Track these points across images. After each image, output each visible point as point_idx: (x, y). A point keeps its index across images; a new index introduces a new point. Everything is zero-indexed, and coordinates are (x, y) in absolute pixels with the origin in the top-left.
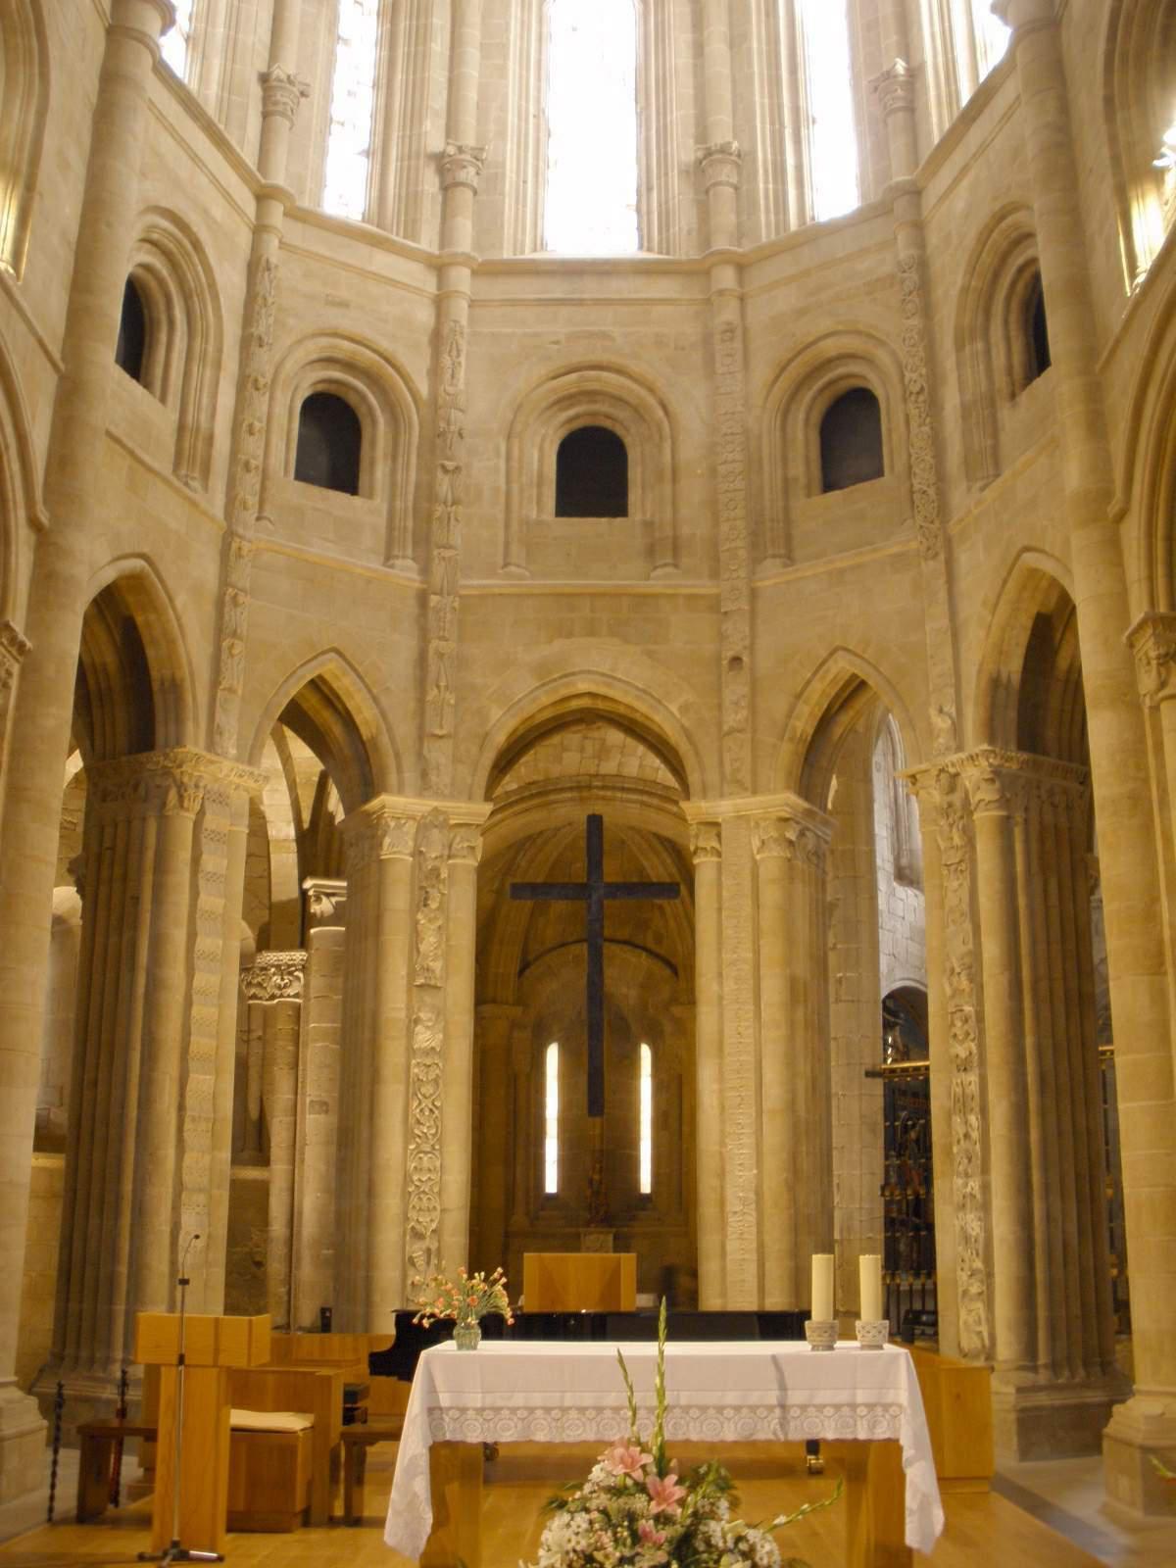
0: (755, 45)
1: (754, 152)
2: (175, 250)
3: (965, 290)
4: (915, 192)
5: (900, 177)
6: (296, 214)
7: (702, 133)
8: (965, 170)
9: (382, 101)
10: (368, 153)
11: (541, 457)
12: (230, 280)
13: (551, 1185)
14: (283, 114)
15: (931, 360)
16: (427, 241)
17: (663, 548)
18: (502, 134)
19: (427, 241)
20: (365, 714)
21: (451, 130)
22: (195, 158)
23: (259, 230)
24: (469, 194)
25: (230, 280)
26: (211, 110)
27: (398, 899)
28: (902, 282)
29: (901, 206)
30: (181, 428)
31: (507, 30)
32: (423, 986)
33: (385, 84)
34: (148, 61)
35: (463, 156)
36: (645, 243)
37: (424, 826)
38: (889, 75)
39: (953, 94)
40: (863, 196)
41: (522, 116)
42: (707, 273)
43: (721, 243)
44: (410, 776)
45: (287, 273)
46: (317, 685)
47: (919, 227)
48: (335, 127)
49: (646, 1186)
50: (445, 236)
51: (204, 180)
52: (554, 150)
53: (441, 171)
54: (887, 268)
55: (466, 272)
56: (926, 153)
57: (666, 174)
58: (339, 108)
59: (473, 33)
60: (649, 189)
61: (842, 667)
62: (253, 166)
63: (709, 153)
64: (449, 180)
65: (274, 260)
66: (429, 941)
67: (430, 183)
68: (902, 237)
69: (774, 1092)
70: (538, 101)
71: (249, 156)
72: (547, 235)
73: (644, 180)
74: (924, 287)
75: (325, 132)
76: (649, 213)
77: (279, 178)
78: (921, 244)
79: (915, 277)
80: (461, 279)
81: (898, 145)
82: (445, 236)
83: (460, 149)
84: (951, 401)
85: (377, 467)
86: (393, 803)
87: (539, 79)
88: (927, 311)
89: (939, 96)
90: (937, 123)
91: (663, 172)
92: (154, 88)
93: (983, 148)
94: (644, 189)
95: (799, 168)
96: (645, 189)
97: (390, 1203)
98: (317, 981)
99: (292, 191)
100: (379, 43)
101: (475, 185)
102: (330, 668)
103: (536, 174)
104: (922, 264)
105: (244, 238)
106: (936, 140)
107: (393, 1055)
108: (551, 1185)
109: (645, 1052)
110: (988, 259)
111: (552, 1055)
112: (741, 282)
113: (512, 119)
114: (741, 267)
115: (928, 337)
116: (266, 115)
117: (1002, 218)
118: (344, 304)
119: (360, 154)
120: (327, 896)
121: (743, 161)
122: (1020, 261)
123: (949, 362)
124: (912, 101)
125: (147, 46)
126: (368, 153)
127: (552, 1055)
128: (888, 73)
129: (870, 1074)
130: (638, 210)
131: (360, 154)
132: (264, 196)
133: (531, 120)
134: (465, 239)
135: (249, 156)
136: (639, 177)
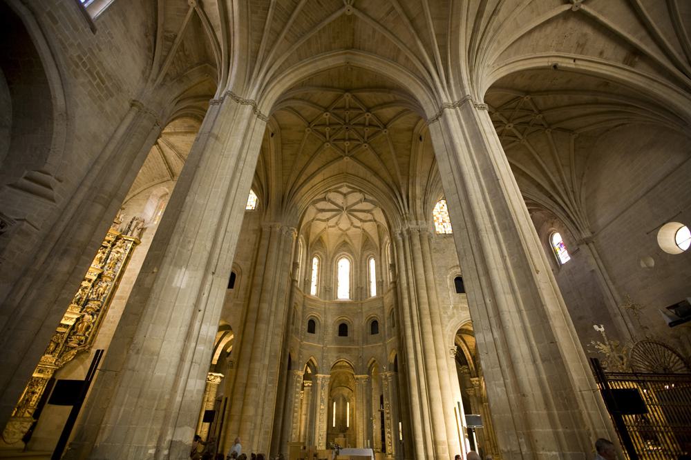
11: (337, 328)
13: (334, 426)
15: (384, 320)
17: (352, 341)
20: (316, 364)
23: (304, 301)
27: (319, 388)
30: (296, 329)
32: (322, 401)
33: (318, 276)
36: (350, 298)
37: (323, 378)
44: (321, 372)
46: (311, 360)
49: (348, 426)
61: (373, 359)
66: (323, 394)
69: (365, 416)
84: (386, 326)
85: (317, 330)
86: (320, 376)
88: (384, 313)
96: (350, 290)
97: (317, 431)
98: (305, 396)
102: (312, 358)
104: (383, 307)
107: (318, 410)
108: (334, 426)
109: (348, 404)
111: (335, 403)
115: (384, 317)
120: (308, 383)
123: (386, 321)
127: (335, 403)
129: (379, 411)
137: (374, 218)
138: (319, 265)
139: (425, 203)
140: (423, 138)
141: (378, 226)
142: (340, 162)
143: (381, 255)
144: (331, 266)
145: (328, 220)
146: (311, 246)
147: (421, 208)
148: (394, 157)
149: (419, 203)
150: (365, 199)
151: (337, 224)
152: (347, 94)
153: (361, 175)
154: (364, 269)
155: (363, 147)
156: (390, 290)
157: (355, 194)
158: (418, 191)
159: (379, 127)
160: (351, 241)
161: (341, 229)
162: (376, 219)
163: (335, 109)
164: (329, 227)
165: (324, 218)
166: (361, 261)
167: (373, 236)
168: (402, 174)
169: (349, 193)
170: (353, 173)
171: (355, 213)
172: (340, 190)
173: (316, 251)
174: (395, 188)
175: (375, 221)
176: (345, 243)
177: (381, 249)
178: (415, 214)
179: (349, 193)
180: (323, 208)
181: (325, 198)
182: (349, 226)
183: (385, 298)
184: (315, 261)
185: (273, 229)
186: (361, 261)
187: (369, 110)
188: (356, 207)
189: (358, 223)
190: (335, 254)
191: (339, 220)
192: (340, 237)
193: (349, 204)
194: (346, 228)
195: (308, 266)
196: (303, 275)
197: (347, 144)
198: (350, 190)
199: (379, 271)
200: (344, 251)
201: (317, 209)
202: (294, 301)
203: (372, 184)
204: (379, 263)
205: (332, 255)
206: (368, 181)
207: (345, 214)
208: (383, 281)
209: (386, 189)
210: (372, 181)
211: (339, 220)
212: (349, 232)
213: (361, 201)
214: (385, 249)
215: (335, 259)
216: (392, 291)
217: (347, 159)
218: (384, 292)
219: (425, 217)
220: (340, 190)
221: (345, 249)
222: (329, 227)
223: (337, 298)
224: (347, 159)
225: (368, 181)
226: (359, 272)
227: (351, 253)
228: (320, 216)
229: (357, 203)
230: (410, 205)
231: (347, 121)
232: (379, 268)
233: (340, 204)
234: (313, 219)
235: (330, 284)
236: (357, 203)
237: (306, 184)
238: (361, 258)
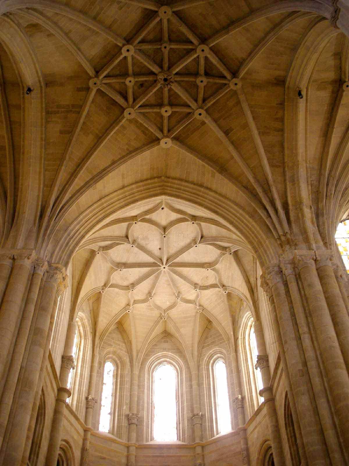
0: (205, 386)
1: (205, 415)
2: (66, 449)
3: (258, 458)
4: (245, 430)
5: (241, 426)
6: (93, 435)
7: (192, 411)
8: (256, 427)
9: (113, 400)
10: (110, 414)
12: (77, 454)
14: (91, 408)
16: (124, 441)
18: (143, 409)
19: (124, 441)
21: (130, 409)
22: (72, 424)
23: (85, 440)
24: (135, 426)
25: (77, 454)
26: (74, 409)
28: (243, 454)
29: (241, 433)
31: (144, 381)
33: (114, 395)
34: (64, 406)
35: (134, 416)
36: (179, 438)
38: (237, 398)
39: (253, 406)
40: (233, 428)
41: (148, 403)
42: (195, 448)
43: (197, 441)
45: (91, 451)
47: (246, 439)
48: (102, 407)
50: (129, 439)
51: (73, 430)
52: (156, 411)
53: (129, 420)
54: (238, 450)
55: (135, 448)
56: (247, 420)
57: (184, 420)
58: (103, 403)
59: (136, 382)
60: (180, 423)
62: (83, 423)
63: (194, 416)
64: (130, 422)
65: (88, 448)
67: (125, 423)
68: (242, 442)
70: (152, 400)
71: (82, 420)
72: (154, 437)
73: (178, 421)
74: (248, 456)
75: (100, 409)
76: (180, 430)
77: (90, 426)
78: (246, 443)
79: (245, 452)
80: (133, 449)
81: (240, 417)
82: (129, 439)
83: (133, 414)
87: (152, 393)
89: (249, 405)
90: (249, 413)
91: (183, 420)
92: (65, 411)
93: (260, 423)
94: (178, 423)
95: (216, 419)
96: (178, 423)
99: (93, 429)
100: (113, 384)
101: (136, 423)
103: (151, 419)
104: (247, 449)
105: (81, 443)
106: (250, 418)
110: (263, 451)
112: (203, 451)
113: (146, 405)
114: (203, 447)
116: (87, 408)
117: (266, 442)
118: (104, 458)
119: (108, 414)
121: (203, 416)
122: (270, 453)
124: (243, 405)
125: (64, 402)
126: (110, 414)
128: (237, 398)
130: (177, 428)
131: (108, 414)
132: (86, 431)
133: (150, 404)
134: (133, 441)
135: (82, 420)
136: (177, 420)
137: (220, 280)
138: (116, 376)
139: (318, 214)
140: (304, 93)
141: (229, 295)
142: (155, 148)
143: (236, 351)
144: (139, 377)
145: (133, 285)
146: (101, 339)
147: (313, 223)
148: (255, 132)
149: (308, 214)
150: (202, 237)
151: (150, 294)
152: (164, 8)
153: (194, 177)
154: (205, 382)
155: (196, 116)
156: (260, 409)
157: (183, 224)
158: (305, 193)
159: (224, 77)
160: (178, 329)
161: (158, 308)
162: (225, 283)
163: (143, 41)
164: (135, 302)
165: (125, 283)
166: (199, 366)
167: (220, 317)
168: (272, 165)
169: (173, 223)
170: (178, 175)
171: (185, 271)
172: (154, 216)
173: (111, 349)
174: (259, 191)
175: (223, 286)
176: (167, 335)
177: (236, 339)
178: (304, 232)
179: (173, 223)
180: (124, 261)
181: (127, 237)
182: (173, 299)
183: (250, 429)
184: (109, 367)
185: (17, 263)
186: (199, 366)
187: (203, 40)
188: (186, 257)
189: (191, 294)
190: (147, 355)
191: (153, 286)
192: (157, 323)
193: (173, 250)
194: (168, 304)
195: (95, 374)
196: (85, 389)
197: (166, 112)
198: (175, 216)
199: (235, 381)
200: (164, 350)
201: (113, 262)
202: (61, 435)
203: (216, 192)
204: (233, 365)
205: (142, 356)
206: (207, 188)
207: (165, 269)
208: (243, 398)
209: (242, 197)
210: (214, 187)
211: (153, 286)
212: (173, 313)
213: (194, 242)
214: (244, 338)
215: (148, 364)
216: (265, 410)
217: (166, 143)
218: (247, 420)
219: (323, 239)
220: (154, 216)
221: (166, 345)
222: (135, 302)
223: (152, 439)
224: (166, 143)
225: (207, 188)
226: (195, 386)
227: (179, 351)
228: (118, 277)
229: (187, 247)
230: (292, 218)
231: (166, 66)
232: (234, 375)
233: (157, 253)
234: (105, 285)
235: (138, 411)
236: (187, 247)
237: (88, 188)
238: (199, 362)
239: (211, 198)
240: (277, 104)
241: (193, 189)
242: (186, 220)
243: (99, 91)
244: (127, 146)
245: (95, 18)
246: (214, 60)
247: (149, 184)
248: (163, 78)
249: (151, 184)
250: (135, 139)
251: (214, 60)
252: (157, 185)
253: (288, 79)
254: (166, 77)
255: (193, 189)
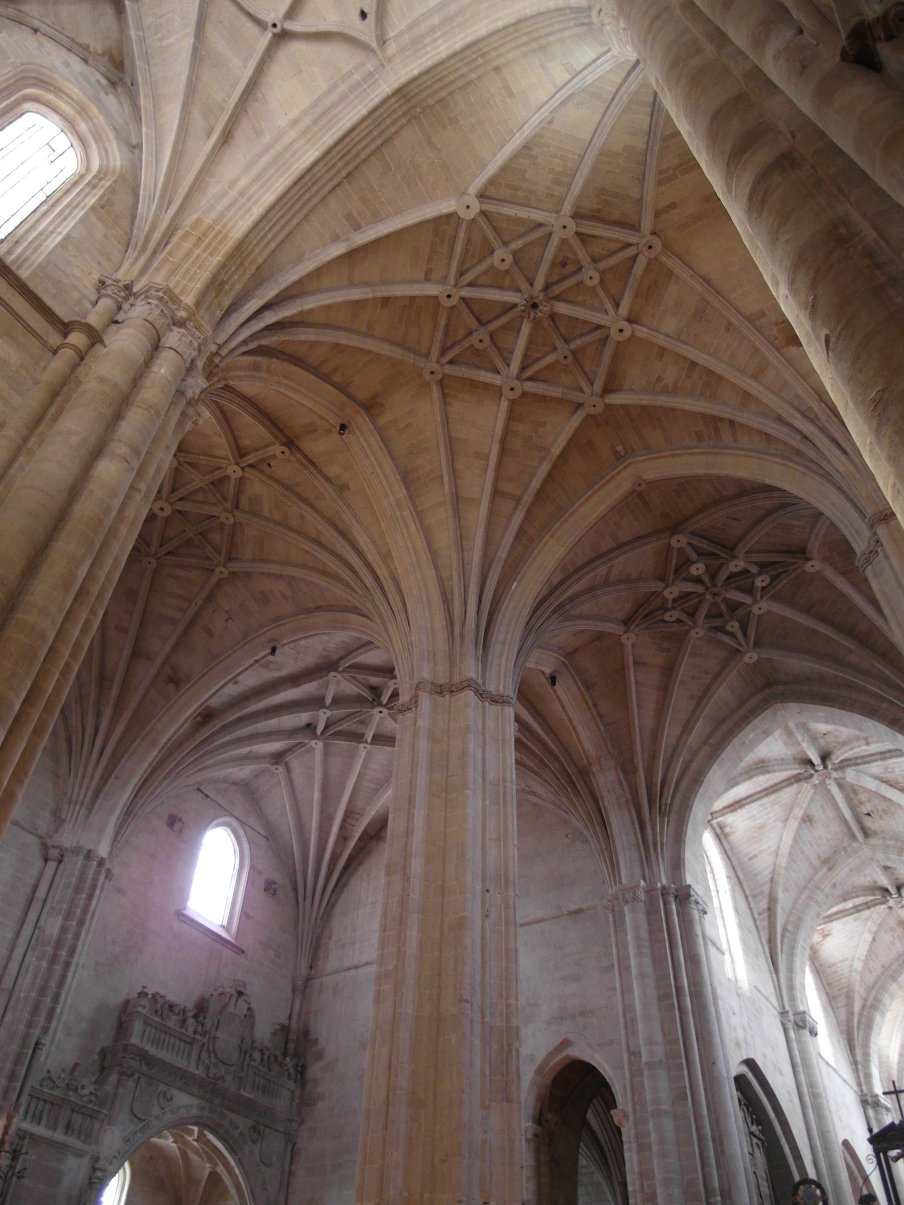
239: (321, 183)
240: (352, 381)
241: (358, 154)
242: (291, 14)
243: (634, 227)
244: (534, 153)
245: (693, 364)
246: (486, 377)
247: (441, 88)
248: (541, 307)
249: (436, 92)
250: (526, 171)
251: (486, 377)
252: (424, 95)
253: (367, 419)
254: (537, 311)
255: (358, 154)
